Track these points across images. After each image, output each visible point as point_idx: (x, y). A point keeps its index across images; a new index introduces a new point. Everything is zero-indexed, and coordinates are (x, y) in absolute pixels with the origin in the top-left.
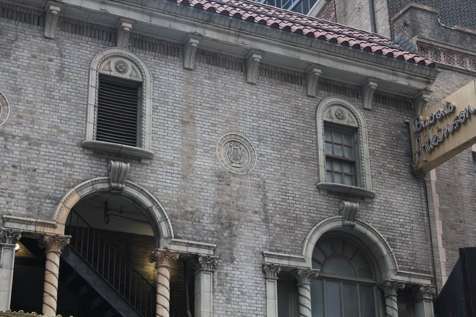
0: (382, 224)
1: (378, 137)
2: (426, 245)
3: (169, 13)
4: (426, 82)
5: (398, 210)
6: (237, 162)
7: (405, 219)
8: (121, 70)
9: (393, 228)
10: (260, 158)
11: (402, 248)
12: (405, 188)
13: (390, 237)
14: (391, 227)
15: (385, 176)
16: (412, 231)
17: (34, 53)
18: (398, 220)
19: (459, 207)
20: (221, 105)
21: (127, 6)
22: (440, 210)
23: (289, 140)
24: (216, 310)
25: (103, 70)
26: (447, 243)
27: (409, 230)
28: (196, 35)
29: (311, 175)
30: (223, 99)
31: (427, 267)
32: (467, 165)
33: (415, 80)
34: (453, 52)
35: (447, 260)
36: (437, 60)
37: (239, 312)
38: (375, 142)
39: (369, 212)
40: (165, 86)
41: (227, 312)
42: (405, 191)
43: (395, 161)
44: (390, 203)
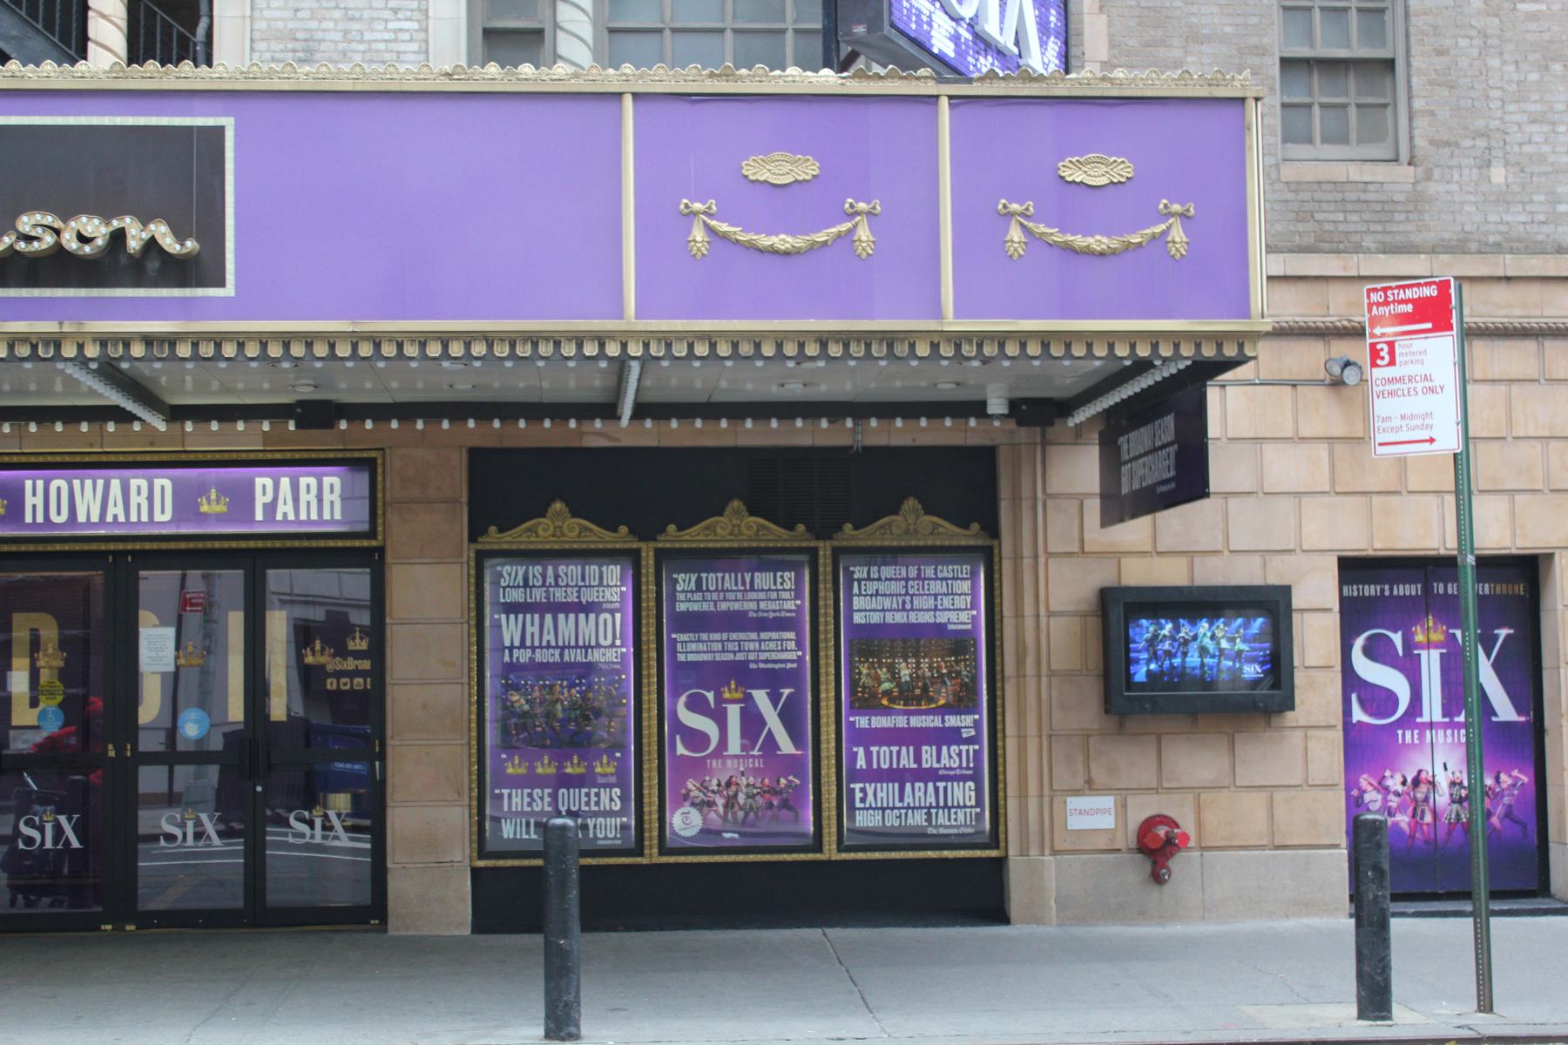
24: (261, 10)
37: (337, 7)
41: (297, 10)
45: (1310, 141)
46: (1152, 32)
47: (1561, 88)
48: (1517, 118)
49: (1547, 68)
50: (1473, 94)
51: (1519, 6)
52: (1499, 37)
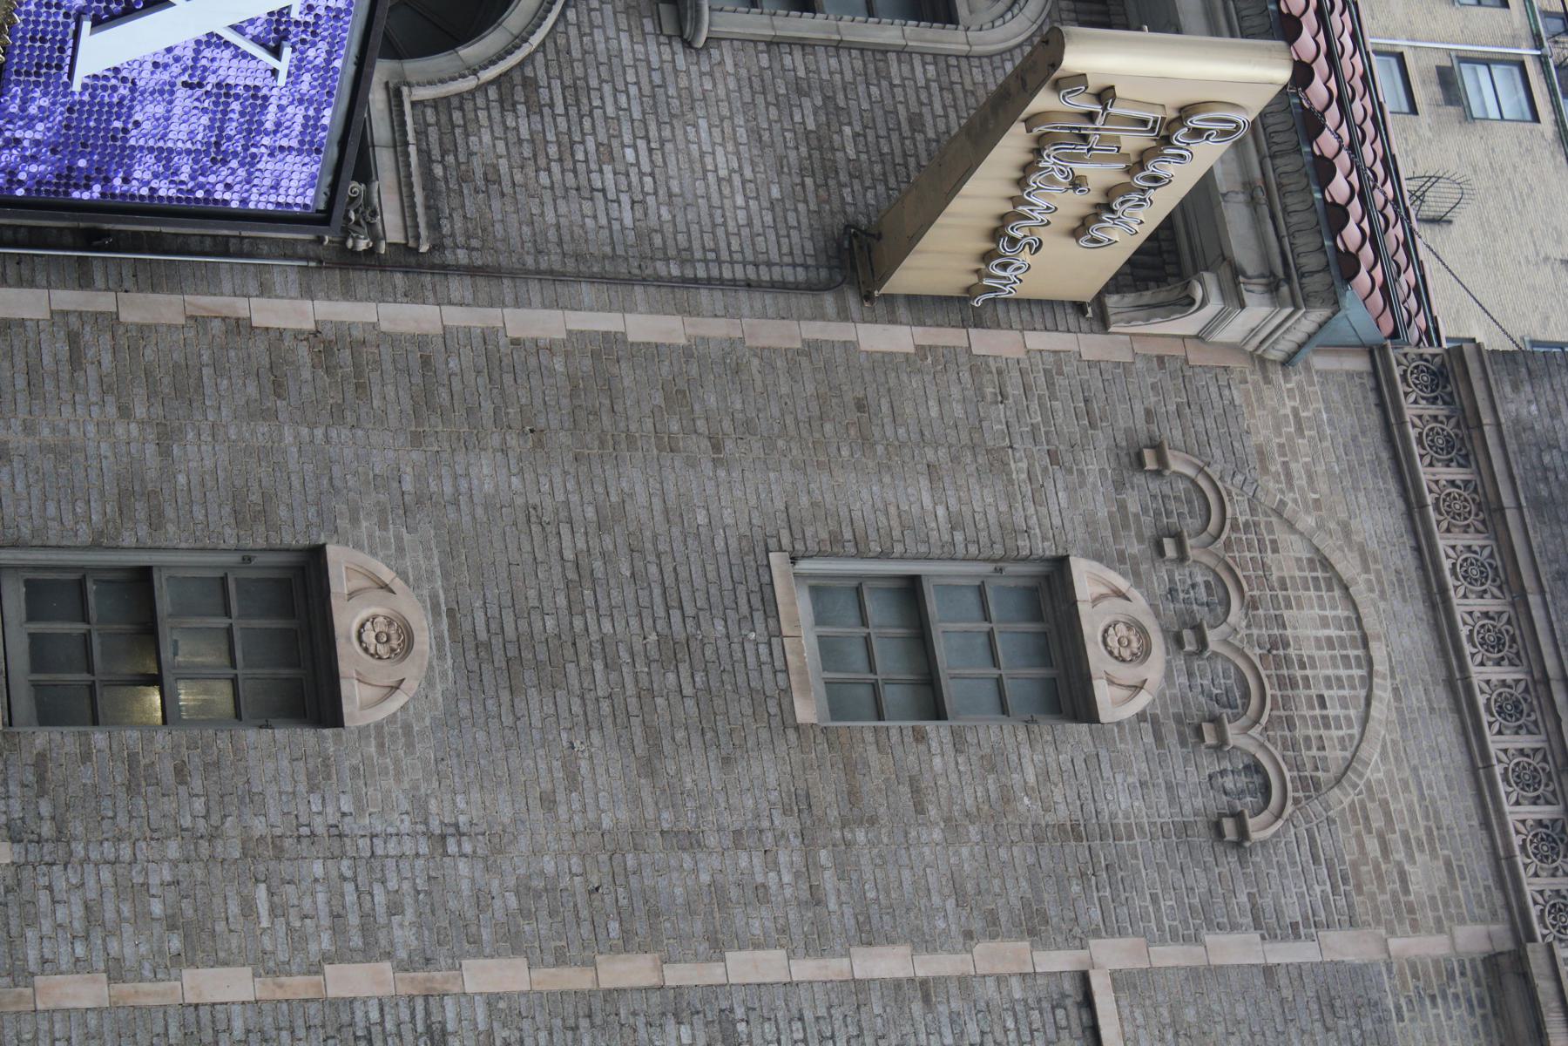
0: (583, 60)
1: (955, 107)
2: (553, 248)
4: (1272, 274)
5: (669, 147)
7: (641, 174)
9: (585, 109)
11: (512, 137)
12: (775, 192)
13: (544, 92)
14: (585, 100)
15: (796, 111)
16: (599, 195)
18: (627, 139)
19: (781, 443)
22: (732, 341)
27: (599, 185)
31: (461, 240)
32: (992, 519)
33: (1256, 221)
34: (1500, 528)
35: (516, 342)
36: (1506, 780)
38: (927, 87)
39: (622, 19)
42: (763, 192)
43: (877, 168)
44: (690, 116)
45: (31, 617)
46: (166, 381)
47: (143, 949)
48: (91, 882)
49: (172, 927)
50: (122, 819)
51: (263, 886)
52: (212, 857)
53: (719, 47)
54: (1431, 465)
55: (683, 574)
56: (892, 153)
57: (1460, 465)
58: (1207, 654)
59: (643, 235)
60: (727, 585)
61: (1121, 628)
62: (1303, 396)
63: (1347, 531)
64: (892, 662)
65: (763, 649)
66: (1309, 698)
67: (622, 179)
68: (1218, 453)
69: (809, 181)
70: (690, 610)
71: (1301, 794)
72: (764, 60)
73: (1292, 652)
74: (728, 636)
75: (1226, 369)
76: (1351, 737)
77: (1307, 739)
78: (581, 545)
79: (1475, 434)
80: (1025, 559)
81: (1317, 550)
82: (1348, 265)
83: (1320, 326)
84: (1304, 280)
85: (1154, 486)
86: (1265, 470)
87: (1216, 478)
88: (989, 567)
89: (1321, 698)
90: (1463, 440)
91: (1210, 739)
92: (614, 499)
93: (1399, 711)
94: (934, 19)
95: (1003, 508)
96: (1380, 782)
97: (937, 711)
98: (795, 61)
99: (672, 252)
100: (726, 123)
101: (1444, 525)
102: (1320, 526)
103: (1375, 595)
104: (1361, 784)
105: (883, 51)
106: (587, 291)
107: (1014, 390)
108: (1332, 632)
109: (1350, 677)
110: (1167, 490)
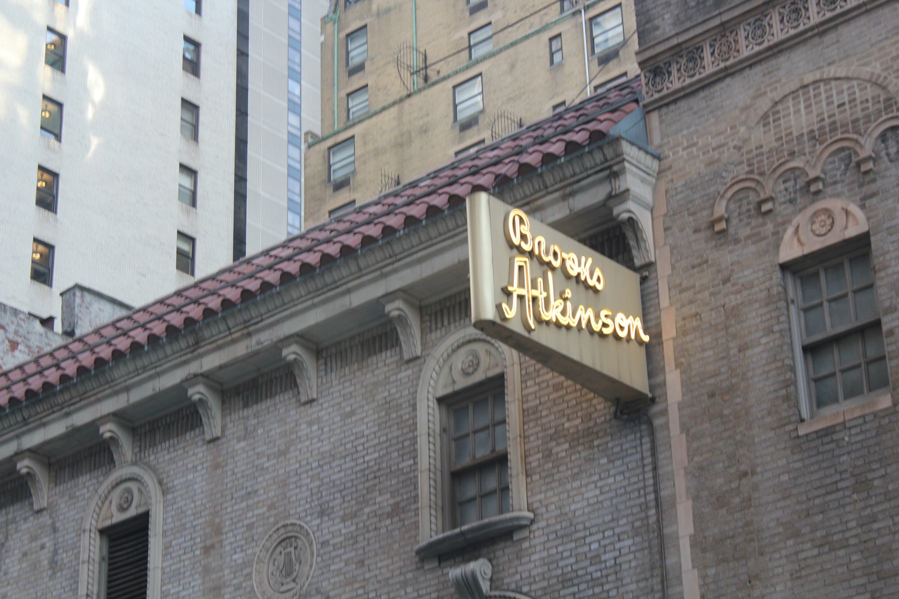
0: (548, 580)
3: (145, 369)
4: (609, 177)
5: (587, 524)
6: (289, 580)
7: (604, 538)
8: (125, 506)
9: (574, 575)
10: (322, 551)
14: (569, 576)
17: (25, 549)
18: (586, 549)
19: (738, 438)
20: (260, 479)
21: (93, 399)
22: (686, 474)
23: (371, 483)
25: (105, 519)
26: (704, 551)
27: (613, 562)
28: (191, 379)
29: (410, 538)
30: (266, 465)
32: (765, 310)
33: (582, 190)
38: (539, 384)
40: (182, 496)
44: (570, 515)
53: (532, 504)
54: (704, 68)
55: (818, 484)
56: (576, 398)
57: (702, 51)
58: (822, 176)
59: (636, 532)
60: (820, 457)
61: (816, 226)
62: (675, 147)
63: (745, 108)
64: (853, 354)
65: (853, 431)
66: (840, 113)
67: (608, 549)
68: (712, 189)
69: (596, 443)
70: (838, 477)
71: (895, 108)
72: (536, 477)
73: (816, 127)
74: (849, 453)
75: (666, 192)
76: (858, 85)
77: (863, 110)
78: (809, 545)
79: (684, 46)
80: (785, 288)
81: (758, 123)
82: (597, 137)
83: (632, 144)
84: (609, 157)
85: (734, 222)
86: (718, 160)
87: (725, 188)
88: (793, 308)
89: (839, 106)
90: (689, 52)
91: (870, 165)
92: (781, 529)
93: (841, 60)
94: (502, 386)
95: (757, 305)
96: (882, 64)
97: (876, 325)
98: (534, 460)
99: (643, 515)
100: (571, 494)
101: (736, 54)
102: (744, 123)
103: (778, 85)
104: (886, 74)
105: (525, 412)
106: (670, 561)
107: (692, 309)
108: (802, 106)
109: (826, 91)
110: (735, 214)
